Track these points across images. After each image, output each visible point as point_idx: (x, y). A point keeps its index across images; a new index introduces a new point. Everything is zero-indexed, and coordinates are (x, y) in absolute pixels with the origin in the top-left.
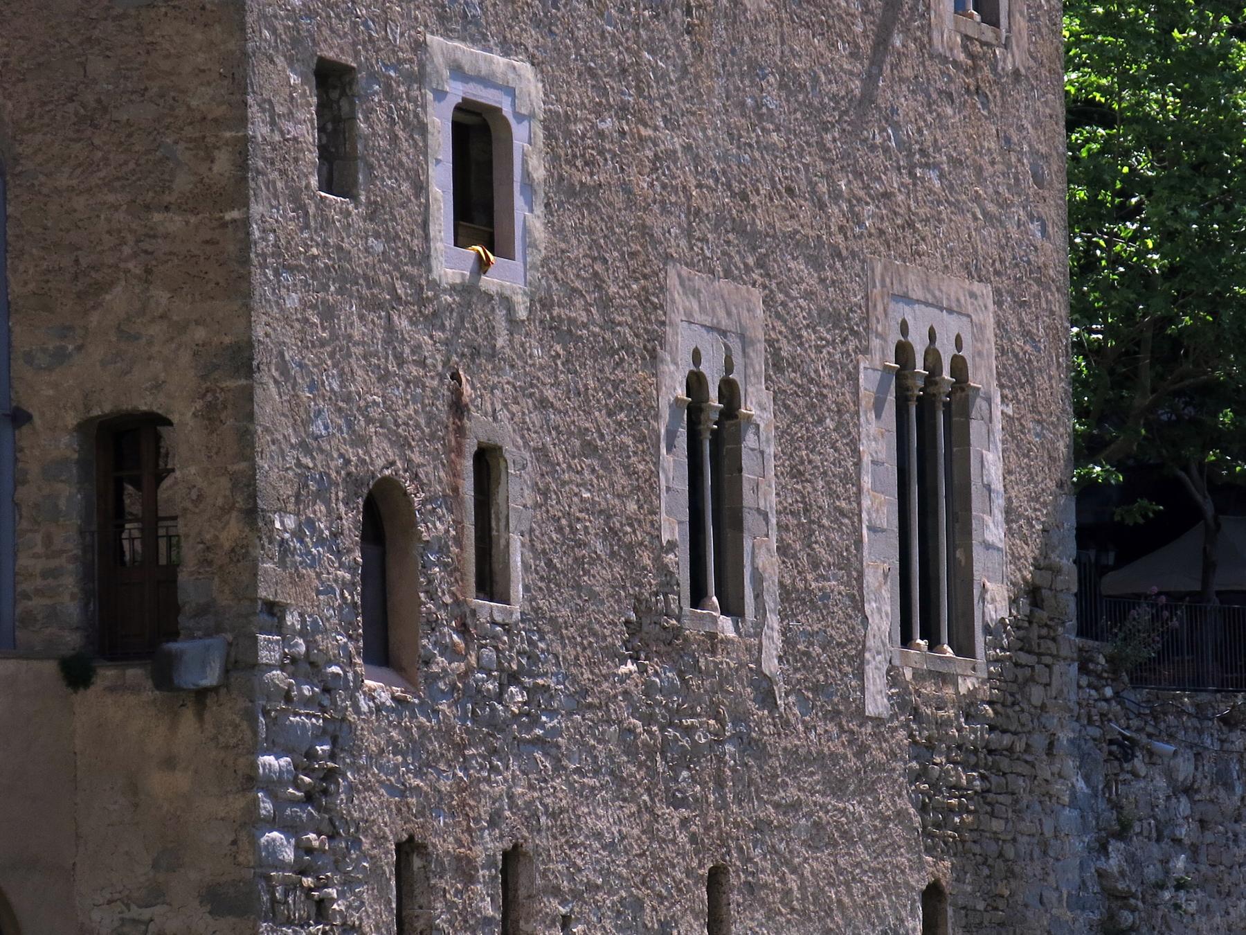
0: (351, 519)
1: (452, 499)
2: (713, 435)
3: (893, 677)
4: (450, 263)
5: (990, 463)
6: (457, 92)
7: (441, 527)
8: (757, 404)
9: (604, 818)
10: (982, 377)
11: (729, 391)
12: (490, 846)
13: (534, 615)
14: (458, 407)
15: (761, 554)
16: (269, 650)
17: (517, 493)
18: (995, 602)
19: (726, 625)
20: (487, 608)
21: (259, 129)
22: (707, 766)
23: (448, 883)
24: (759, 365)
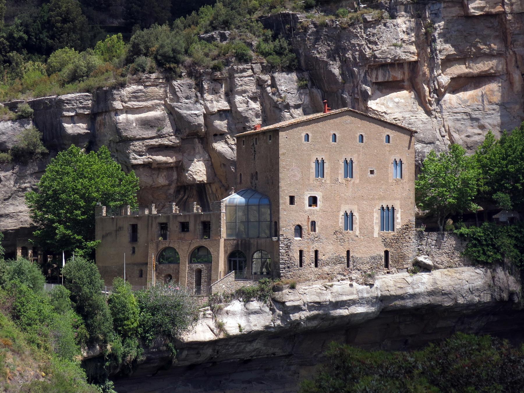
0: (293, 229)
1: (308, 225)
2: (349, 218)
3: (379, 234)
4: (307, 207)
5: (398, 215)
6: (309, 195)
7: (306, 227)
8: (356, 214)
9: (331, 247)
10: (397, 207)
11: (352, 214)
12: (314, 250)
13: (320, 233)
14: (308, 218)
15: (356, 226)
16: (281, 238)
17: (318, 224)
18: (398, 227)
19: (351, 232)
20: (312, 233)
21: (281, 201)
22: (347, 242)
23: (307, 253)
24: (356, 210)
